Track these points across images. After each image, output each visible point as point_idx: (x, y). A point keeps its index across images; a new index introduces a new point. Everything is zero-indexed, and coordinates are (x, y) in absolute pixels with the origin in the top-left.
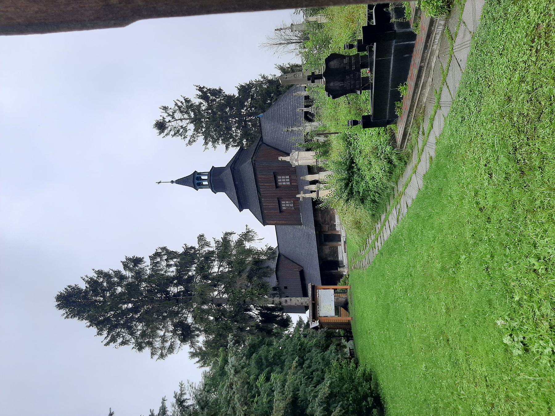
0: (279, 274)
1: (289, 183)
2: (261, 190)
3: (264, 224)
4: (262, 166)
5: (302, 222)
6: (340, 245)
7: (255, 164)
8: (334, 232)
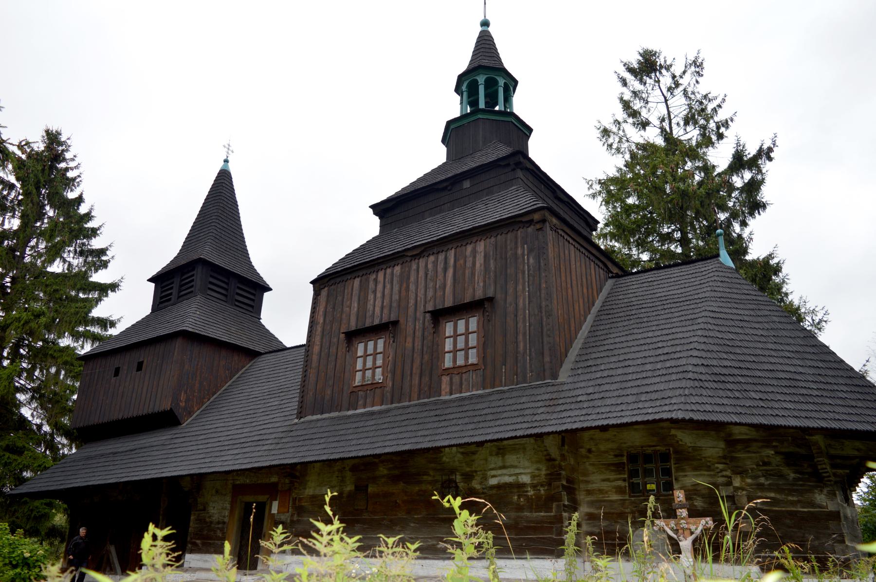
0: (179, 343)
1: (448, 363)
2: (432, 258)
3: (319, 283)
4: (519, 251)
7: (531, 222)
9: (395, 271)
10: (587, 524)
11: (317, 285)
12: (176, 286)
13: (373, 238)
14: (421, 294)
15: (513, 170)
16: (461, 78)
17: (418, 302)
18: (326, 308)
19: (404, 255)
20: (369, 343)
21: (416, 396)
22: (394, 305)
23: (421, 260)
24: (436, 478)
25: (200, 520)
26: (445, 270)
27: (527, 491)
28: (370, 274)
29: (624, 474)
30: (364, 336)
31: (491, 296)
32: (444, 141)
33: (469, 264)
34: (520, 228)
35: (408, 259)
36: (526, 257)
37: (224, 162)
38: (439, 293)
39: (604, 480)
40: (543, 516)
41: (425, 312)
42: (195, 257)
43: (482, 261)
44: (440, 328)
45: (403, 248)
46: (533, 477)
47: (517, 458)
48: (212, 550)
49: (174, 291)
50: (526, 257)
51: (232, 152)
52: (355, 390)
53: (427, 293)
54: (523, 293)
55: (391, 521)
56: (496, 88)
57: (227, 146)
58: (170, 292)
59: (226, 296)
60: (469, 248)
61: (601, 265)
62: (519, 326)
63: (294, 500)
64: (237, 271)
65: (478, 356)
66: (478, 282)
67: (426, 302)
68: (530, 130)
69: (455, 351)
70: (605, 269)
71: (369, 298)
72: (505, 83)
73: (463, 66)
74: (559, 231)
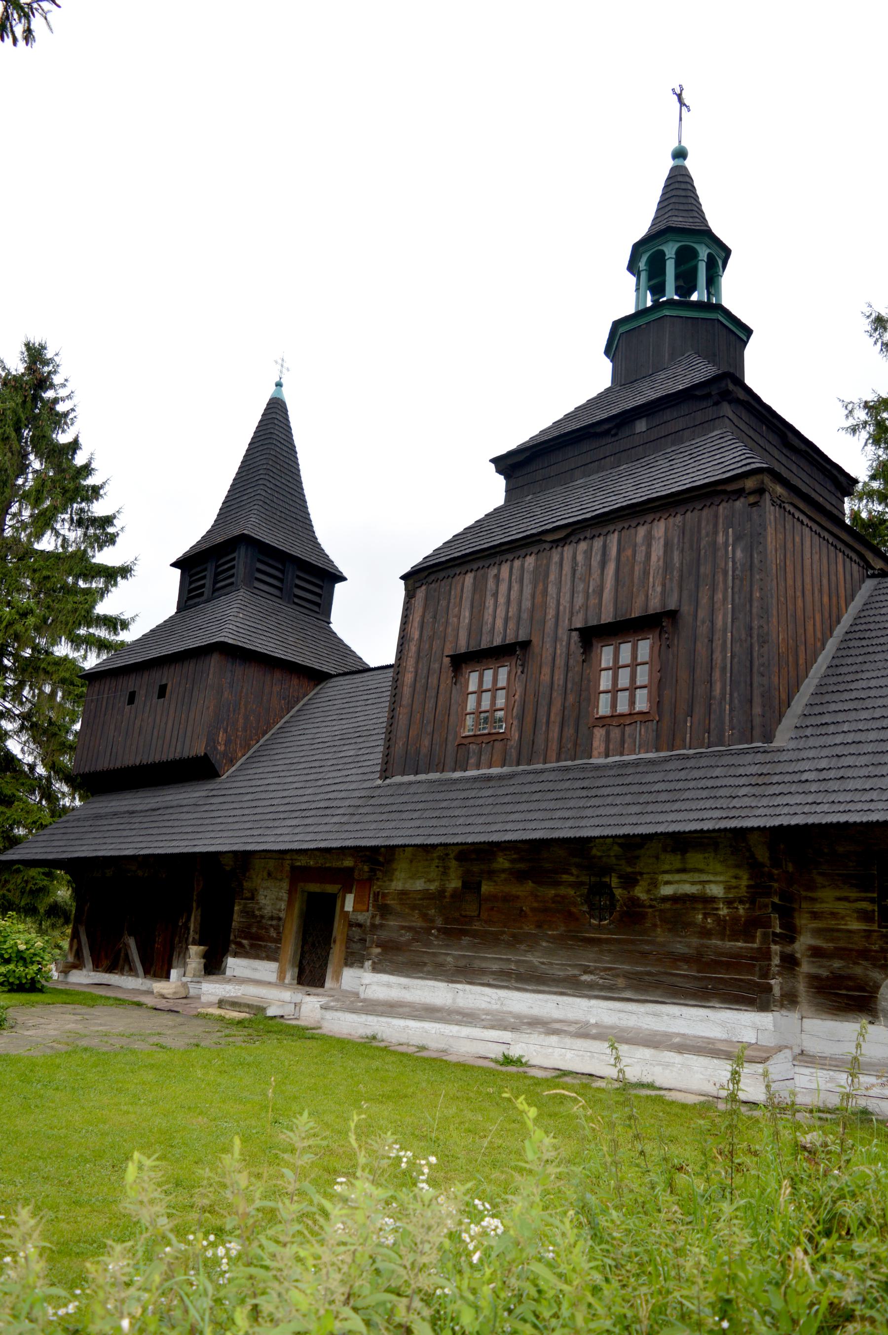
1: (603, 708)
2: (583, 546)
4: (720, 539)
5: (398, 779)
6: (281, 982)
7: (740, 493)
8: (337, 952)
9: (526, 564)
10: (809, 962)
11: (411, 582)
12: (210, 574)
13: (495, 510)
14: (565, 601)
15: (716, 404)
16: (638, 249)
17: (561, 614)
18: (423, 616)
19: (541, 540)
20: (486, 672)
21: (554, 758)
22: (525, 616)
23: (566, 548)
24: (580, 879)
25: (248, 913)
26: (603, 564)
27: (717, 909)
28: (488, 567)
29: (873, 892)
30: (478, 662)
31: (673, 608)
32: (607, 352)
33: (640, 557)
34: (722, 501)
35: (547, 546)
36: (730, 548)
37: (277, 385)
38: (593, 601)
39: (839, 899)
40: (741, 948)
41: (571, 630)
42: (236, 533)
43: (661, 553)
44: (593, 654)
45: (540, 529)
46: (728, 888)
47: (705, 858)
48: (264, 955)
49: (208, 582)
50: (730, 548)
51: (288, 370)
52: (466, 741)
53: (575, 600)
54: (723, 604)
55: (514, 936)
56: (693, 263)
57: (280, 362)
58: (202, 582)
59: (280, 589)
60: (642, 531)
61: (854, 557)
62: (714, 657)
63: (376, 895)
64: (296, 552)
65: (650, 700)
66: (654, 586)
67: (572, 614)
68: (749, 332)
69: (615, 691)
70: (862, 564)
71: (487, 604)
72: (710, 255)
73: (641, 227)
74: (786, 505)
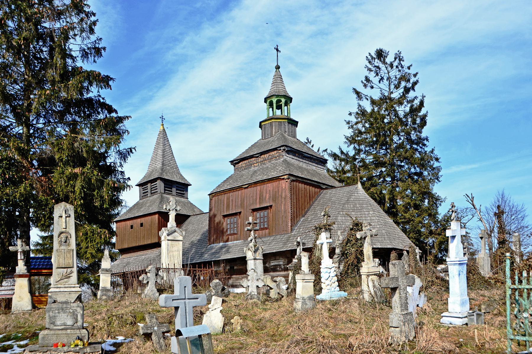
3: (212, 195)
11: (211, 196)
49: (149, 190)
